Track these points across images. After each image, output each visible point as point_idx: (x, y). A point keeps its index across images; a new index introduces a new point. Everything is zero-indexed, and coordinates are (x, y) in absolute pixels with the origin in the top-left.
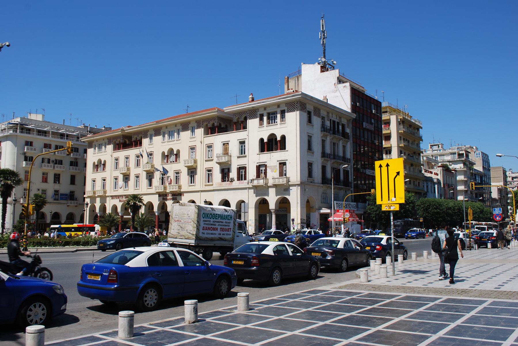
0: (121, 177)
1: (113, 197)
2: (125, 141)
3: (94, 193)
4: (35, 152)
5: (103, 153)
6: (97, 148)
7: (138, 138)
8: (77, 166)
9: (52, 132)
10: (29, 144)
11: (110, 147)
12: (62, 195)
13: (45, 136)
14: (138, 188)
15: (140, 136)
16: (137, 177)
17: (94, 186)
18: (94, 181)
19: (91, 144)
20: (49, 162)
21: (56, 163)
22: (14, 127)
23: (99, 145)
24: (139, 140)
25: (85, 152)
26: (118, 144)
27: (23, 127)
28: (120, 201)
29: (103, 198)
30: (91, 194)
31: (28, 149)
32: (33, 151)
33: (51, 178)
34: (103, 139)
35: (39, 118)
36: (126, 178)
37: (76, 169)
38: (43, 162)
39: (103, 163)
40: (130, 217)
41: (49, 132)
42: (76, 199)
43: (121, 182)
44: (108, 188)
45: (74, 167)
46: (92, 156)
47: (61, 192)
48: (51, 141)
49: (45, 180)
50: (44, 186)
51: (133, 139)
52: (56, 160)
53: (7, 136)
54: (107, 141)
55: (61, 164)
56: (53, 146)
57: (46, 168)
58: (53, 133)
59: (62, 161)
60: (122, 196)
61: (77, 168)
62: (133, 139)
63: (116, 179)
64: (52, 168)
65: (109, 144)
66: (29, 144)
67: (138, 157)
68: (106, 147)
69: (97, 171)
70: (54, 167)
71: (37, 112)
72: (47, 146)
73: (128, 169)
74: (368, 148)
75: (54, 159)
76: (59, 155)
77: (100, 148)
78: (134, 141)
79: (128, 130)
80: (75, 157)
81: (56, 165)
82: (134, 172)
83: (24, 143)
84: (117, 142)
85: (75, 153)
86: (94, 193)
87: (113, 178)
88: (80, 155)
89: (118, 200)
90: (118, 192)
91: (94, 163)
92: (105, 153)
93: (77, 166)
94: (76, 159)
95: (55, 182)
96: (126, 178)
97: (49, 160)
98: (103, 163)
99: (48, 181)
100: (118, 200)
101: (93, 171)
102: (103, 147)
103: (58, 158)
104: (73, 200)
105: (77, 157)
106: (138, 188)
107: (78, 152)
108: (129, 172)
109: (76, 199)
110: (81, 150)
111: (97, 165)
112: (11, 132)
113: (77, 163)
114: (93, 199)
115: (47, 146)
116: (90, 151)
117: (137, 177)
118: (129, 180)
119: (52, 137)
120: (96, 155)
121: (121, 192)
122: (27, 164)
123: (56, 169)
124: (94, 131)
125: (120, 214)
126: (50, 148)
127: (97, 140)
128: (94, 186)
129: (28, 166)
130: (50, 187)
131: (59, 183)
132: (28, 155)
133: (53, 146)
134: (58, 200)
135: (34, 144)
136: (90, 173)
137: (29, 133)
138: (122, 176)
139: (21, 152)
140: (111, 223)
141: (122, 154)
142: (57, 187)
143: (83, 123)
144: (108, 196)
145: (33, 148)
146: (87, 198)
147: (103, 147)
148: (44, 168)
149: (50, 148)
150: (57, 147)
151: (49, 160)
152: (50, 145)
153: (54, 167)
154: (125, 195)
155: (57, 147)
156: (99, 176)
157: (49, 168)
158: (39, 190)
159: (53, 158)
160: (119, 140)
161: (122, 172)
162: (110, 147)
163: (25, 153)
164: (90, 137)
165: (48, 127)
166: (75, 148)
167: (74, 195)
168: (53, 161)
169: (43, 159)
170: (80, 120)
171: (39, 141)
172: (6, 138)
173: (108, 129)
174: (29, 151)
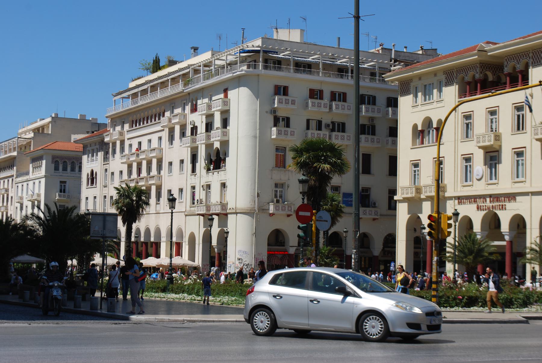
0: (479, 157)
1: (460, 199)
2: (486, 76)
3: (418, 190)
4: (293, 107)
5: (435, 105)
6: (420, 94)
7: (520, 67)
8: (374, 134)
9: (324, 64)
10: (282, 91)
11: (451, 92)
13: (310, 73)
14: (520, 179)
15: (523, 61)
16: (520, 154)
17: (415, 176)
18: (416, 165)
19: (405, 87)
20: (319, 128)
21: (333, 130)
22: (252, 57)
23: (426, 88)
24: (521, 72)
25: (393, 103)
26: (469, 83)
27: (268, 58)
28: (478, 208)
29: (439, 200)
30: (411, 194)
31: (280, 102)
32: (290, 106)
34: (435, 73)
35: (295, 36)
36: (492, 157)
37: (373, 141)
38: (308, 128)
39: (435, 125)
40: (504, 243)
41: (317, 64)
42: (374, 205)
43: (479, 166)
44: (448, 179)
45: (370, 137)
46: (410, 112)
48: (321, 82)
51: (507, 70)
52: (333, 123)
53: (239, 77)
54: (443, 77)
55: (343, 131)
56: (327, 95)
58: (326, 67)
59: (344, 124)
60: (484, 197)
61: (375, 138)
62: (507, 70)
63: (468, 160)
65: (449, 83)
66: (282, 91)
67: (519, 108)
68: (440, 91)
69: (422, 143)
71: (289, 26)
72: (315, 94)
73: (498, 138)
75: (329, 122)
76: (340, 111)
77: (427, 93)
78: (509, 75)
79: (494, 51)
80: (370, 114)
81: (334, 134)
82: (509, 143)
83: (272, 90)
84: (468, 78)
85: (370, 107)
86: (418, 190)
87: (460, 158)
88: (379, 111)
89: (474, 206)
90: (474, 188)
91: (415, 126)
92: (440, 105)
93: (374, 134)
94: (372, 119)
96: (492, 157)
97: (319, 123)
98: (435, 125)
100: (474, 206)
101: (414, 143)
102: (435, 91)
103: (337, 119)
104: (368, 206)
105: (375, 115)
106: (520, 179)
107: (374, 103)
108: (498, 143)
109: (374, 205)
110: (381, 101)
111: (422, 132)
112: (245, 68)
113: (373, 127)
114: (414, 204)
115: (315, 94)
116: (405, 102)
117: (520, 154)
118: (499, 162)
119: (324, 74)
120: (420, 108)
121: (479, 188)
122: (279, 133)
124: (407, 60)
125: (507, 238)
126: (321, 98)
127: (420, 77)
128: (415, 176)
129: (283, 137)
132: (281, 114)
133: (327, 95)
135: (290, 91)
136: (406, 150)
137: (279, 69)
138: (481, 152)
139: (268, 108)
140: (475, 258)
141: (479, 106)
143: (380, 41)
144: (450, 198)
145: (290, 98)
146: (400, 201)
147: (435, 91)
149: (321, 98)
150: (334, 96)
151: (319, 123)
152: (321, 92)
154: (490, 196)
155: (334, 96)
156: (427, 155)
159: (326, 120)
160: (471, 74)
161: (482, 144)
162: (451, 92)
163: (274, 111)
164: (396, 74)
165: (315, 54)
166: (369, 96)
167: (368, 196)
168: (327, 126)
169: (308, 121)
170: (372, 37)
172: (238, 81)
173: (431, 53)
174: (283, 106)
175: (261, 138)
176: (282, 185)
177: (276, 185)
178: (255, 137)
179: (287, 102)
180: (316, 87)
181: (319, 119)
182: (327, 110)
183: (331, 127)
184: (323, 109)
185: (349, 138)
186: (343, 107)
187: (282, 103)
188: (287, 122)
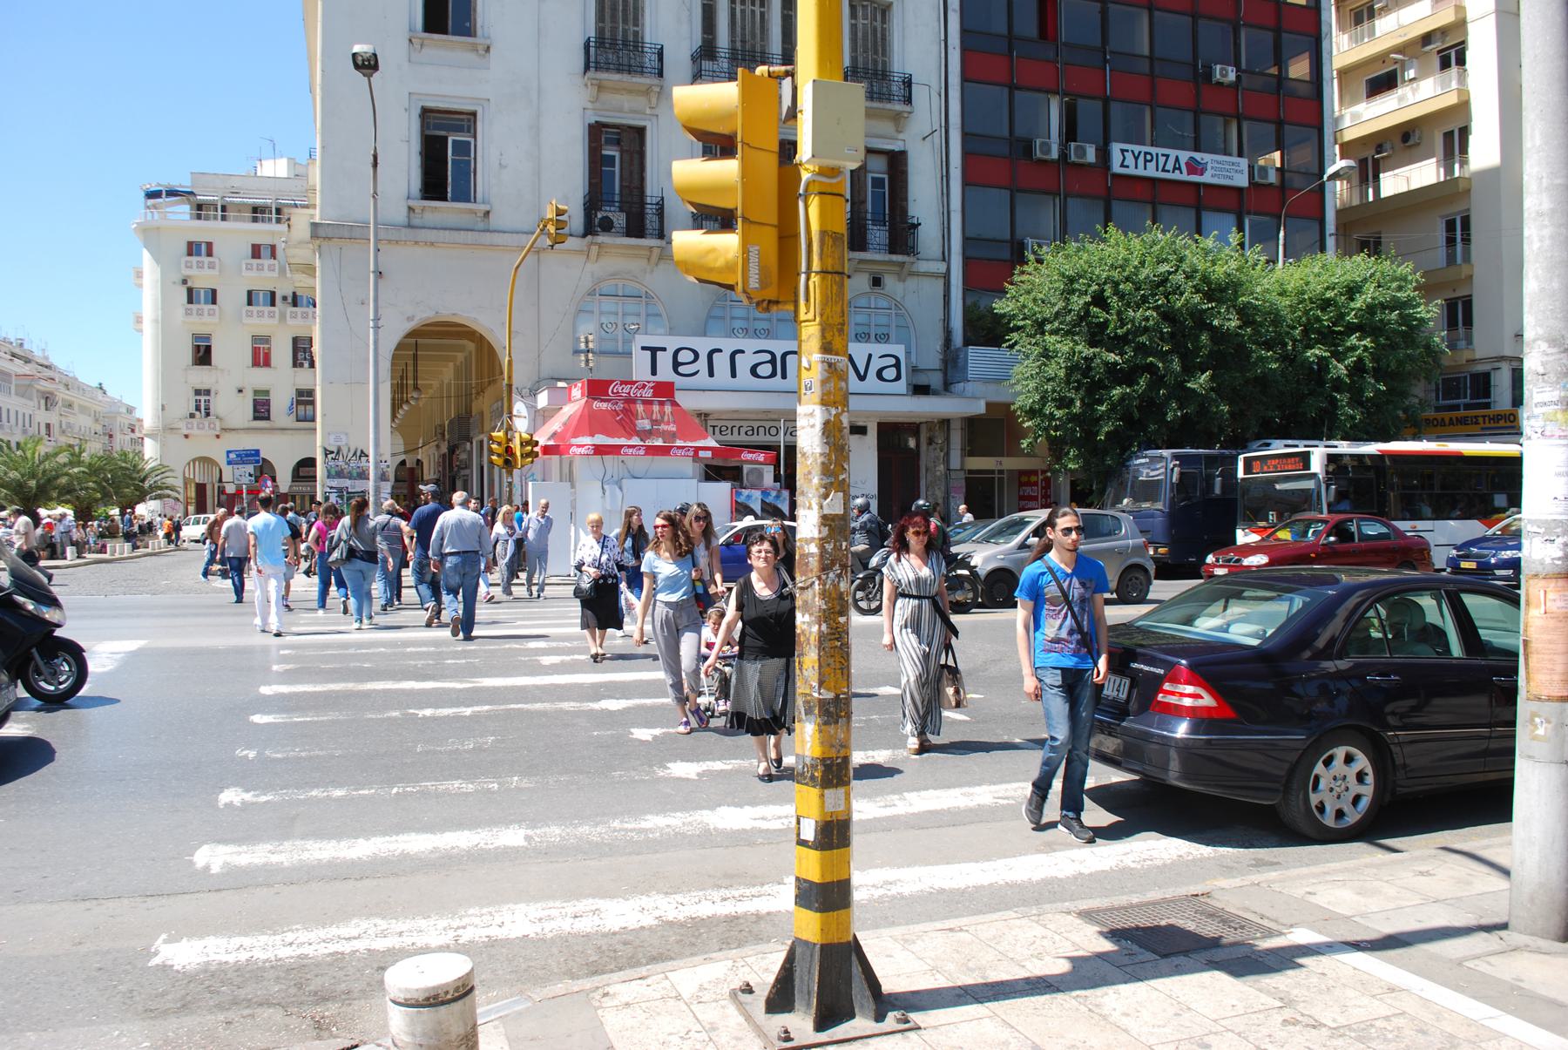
32: (207, 272)
33: (282, 352)
48: (273, 233)
49: (261, 358)
57: (255, 320)
64: (275, 321)
70: (283, 317)
74: (1281, 79)
95: (296, 364)
122: (188, 313)
123: (290, 322)
129: (194, 319)
130: (281, 381)
135: (215, 250)
139: (179, 278)
148: (246, 321)
153: (283, 317)
157: (266, 321)
168: (285, 298)
171: (233, 236)
175: (164, 323)
176: (208, 392)
178: (156, 321)
179: (200, 266)
182: (275, 274)
184: (266, 273)
188: (213, 297)
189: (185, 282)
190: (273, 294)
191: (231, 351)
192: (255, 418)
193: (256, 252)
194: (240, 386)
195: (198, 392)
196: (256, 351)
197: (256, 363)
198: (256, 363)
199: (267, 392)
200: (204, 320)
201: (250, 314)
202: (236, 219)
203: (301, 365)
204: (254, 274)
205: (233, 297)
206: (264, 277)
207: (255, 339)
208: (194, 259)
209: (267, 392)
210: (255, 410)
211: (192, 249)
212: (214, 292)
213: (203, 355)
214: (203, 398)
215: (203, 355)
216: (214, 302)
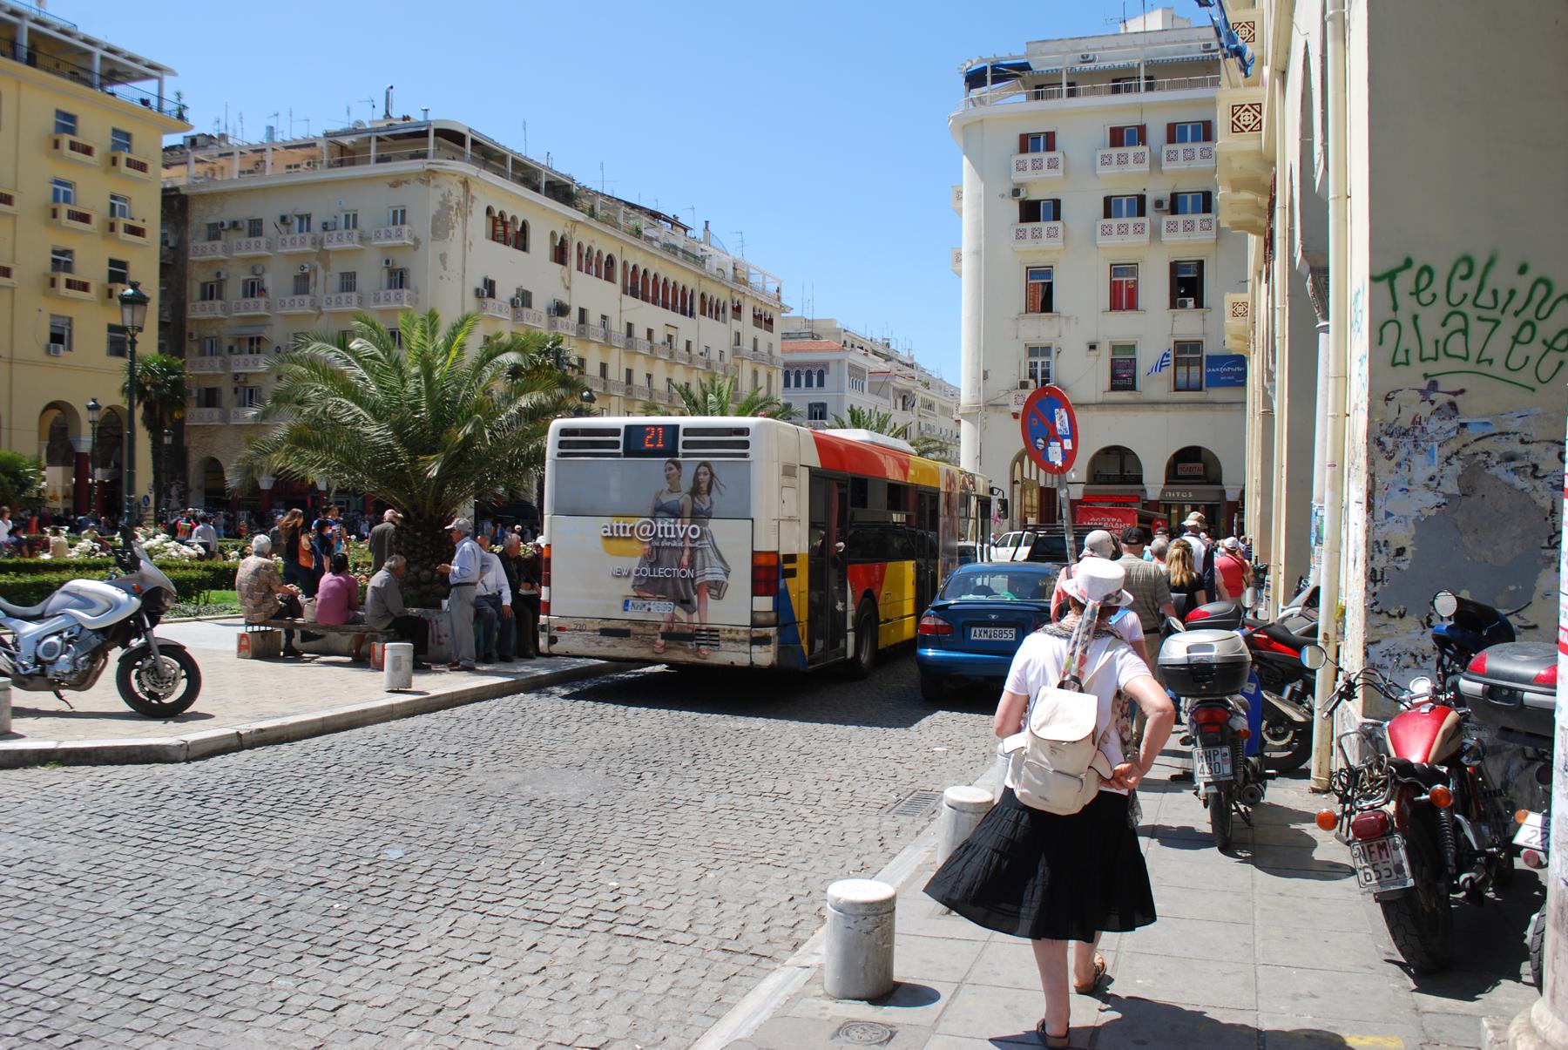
4: (1053, 173)
12: (1214, 360)
32: (1046, 173)
33: (1154, 286)
47: (1210, 349)
48: (1141, 108)
49: (1123, 296)
50: (1122, 326)
56: (1156, 133)
57: (1115, 240)
70: (1156, 233)
75: (1165, 195)
99: (1141, 302)
122: (1020, 236)
123: (1166, 237)
129: (1028, 244)
130: (1155, 327)
131: (1199, 304)
133: (1156, 133)
134: (1200, 389)
135: (1059, 141)
139: (1007, 188)
142: (1188, 323)
148: (1102, 241)
150: (1174, 133)
153: (1156, 233)
157: (1131, 239)
158: (1092, 347)
159: (1158, 190)
168: (1159, 204)
171: (1083, 119)
175: (987, 254)
176: (1046, 351)
177: (1033, 351)
179: (1037, 166)
180: (1128, 120)
181: (1139, 191)
182: (1145, 167)
183: (1166, 205)
184: (1132, 167)
185: (1206, 225)
186: (1189, 154)
187: (1024, 169)
189: (1016, 192)
190: (1141, 199)
191: (1082, 290)
192: (1114, 388)
193: (1117, 137)
194: (1092, 338)
195: (1033, 351)
196: (1115, 288)
197: (1115, 305)
198: (1115, 305)
199: (1131, 348)
200: (1042, 244)
201: (1106, 231)
202: (1087, 93)
203: (1184, 305)
204: (1113, 169)
205: (1082, 209)
206: (1130, 174)
207: (1116, 269)
208: (1029, 157)
209: (1131, 348)
210: (1114, 376)
211: (1027, 143)
212: (1057, 203)
213: (1043, 299)
214: (1039, 361)
215: (1043, 299)
216: (1057, 217)
